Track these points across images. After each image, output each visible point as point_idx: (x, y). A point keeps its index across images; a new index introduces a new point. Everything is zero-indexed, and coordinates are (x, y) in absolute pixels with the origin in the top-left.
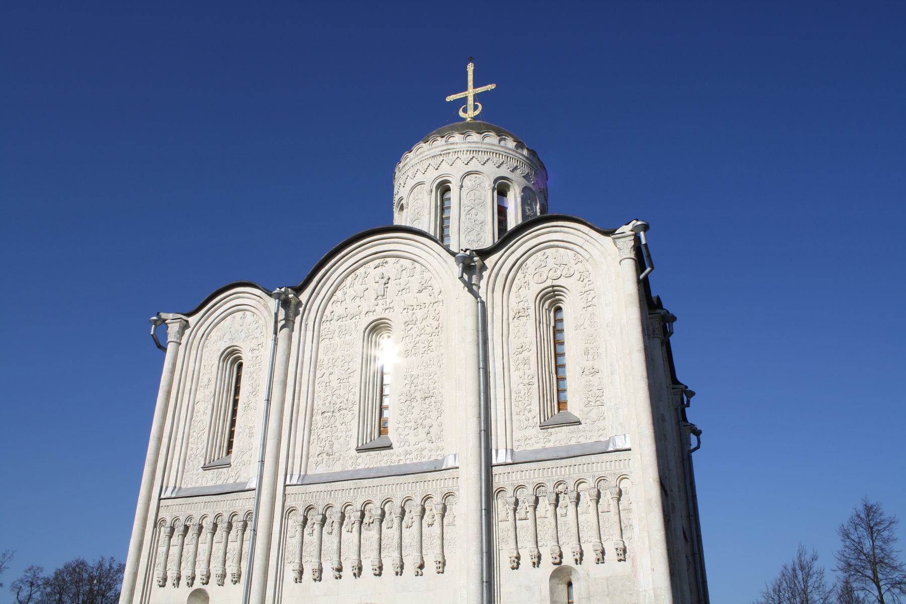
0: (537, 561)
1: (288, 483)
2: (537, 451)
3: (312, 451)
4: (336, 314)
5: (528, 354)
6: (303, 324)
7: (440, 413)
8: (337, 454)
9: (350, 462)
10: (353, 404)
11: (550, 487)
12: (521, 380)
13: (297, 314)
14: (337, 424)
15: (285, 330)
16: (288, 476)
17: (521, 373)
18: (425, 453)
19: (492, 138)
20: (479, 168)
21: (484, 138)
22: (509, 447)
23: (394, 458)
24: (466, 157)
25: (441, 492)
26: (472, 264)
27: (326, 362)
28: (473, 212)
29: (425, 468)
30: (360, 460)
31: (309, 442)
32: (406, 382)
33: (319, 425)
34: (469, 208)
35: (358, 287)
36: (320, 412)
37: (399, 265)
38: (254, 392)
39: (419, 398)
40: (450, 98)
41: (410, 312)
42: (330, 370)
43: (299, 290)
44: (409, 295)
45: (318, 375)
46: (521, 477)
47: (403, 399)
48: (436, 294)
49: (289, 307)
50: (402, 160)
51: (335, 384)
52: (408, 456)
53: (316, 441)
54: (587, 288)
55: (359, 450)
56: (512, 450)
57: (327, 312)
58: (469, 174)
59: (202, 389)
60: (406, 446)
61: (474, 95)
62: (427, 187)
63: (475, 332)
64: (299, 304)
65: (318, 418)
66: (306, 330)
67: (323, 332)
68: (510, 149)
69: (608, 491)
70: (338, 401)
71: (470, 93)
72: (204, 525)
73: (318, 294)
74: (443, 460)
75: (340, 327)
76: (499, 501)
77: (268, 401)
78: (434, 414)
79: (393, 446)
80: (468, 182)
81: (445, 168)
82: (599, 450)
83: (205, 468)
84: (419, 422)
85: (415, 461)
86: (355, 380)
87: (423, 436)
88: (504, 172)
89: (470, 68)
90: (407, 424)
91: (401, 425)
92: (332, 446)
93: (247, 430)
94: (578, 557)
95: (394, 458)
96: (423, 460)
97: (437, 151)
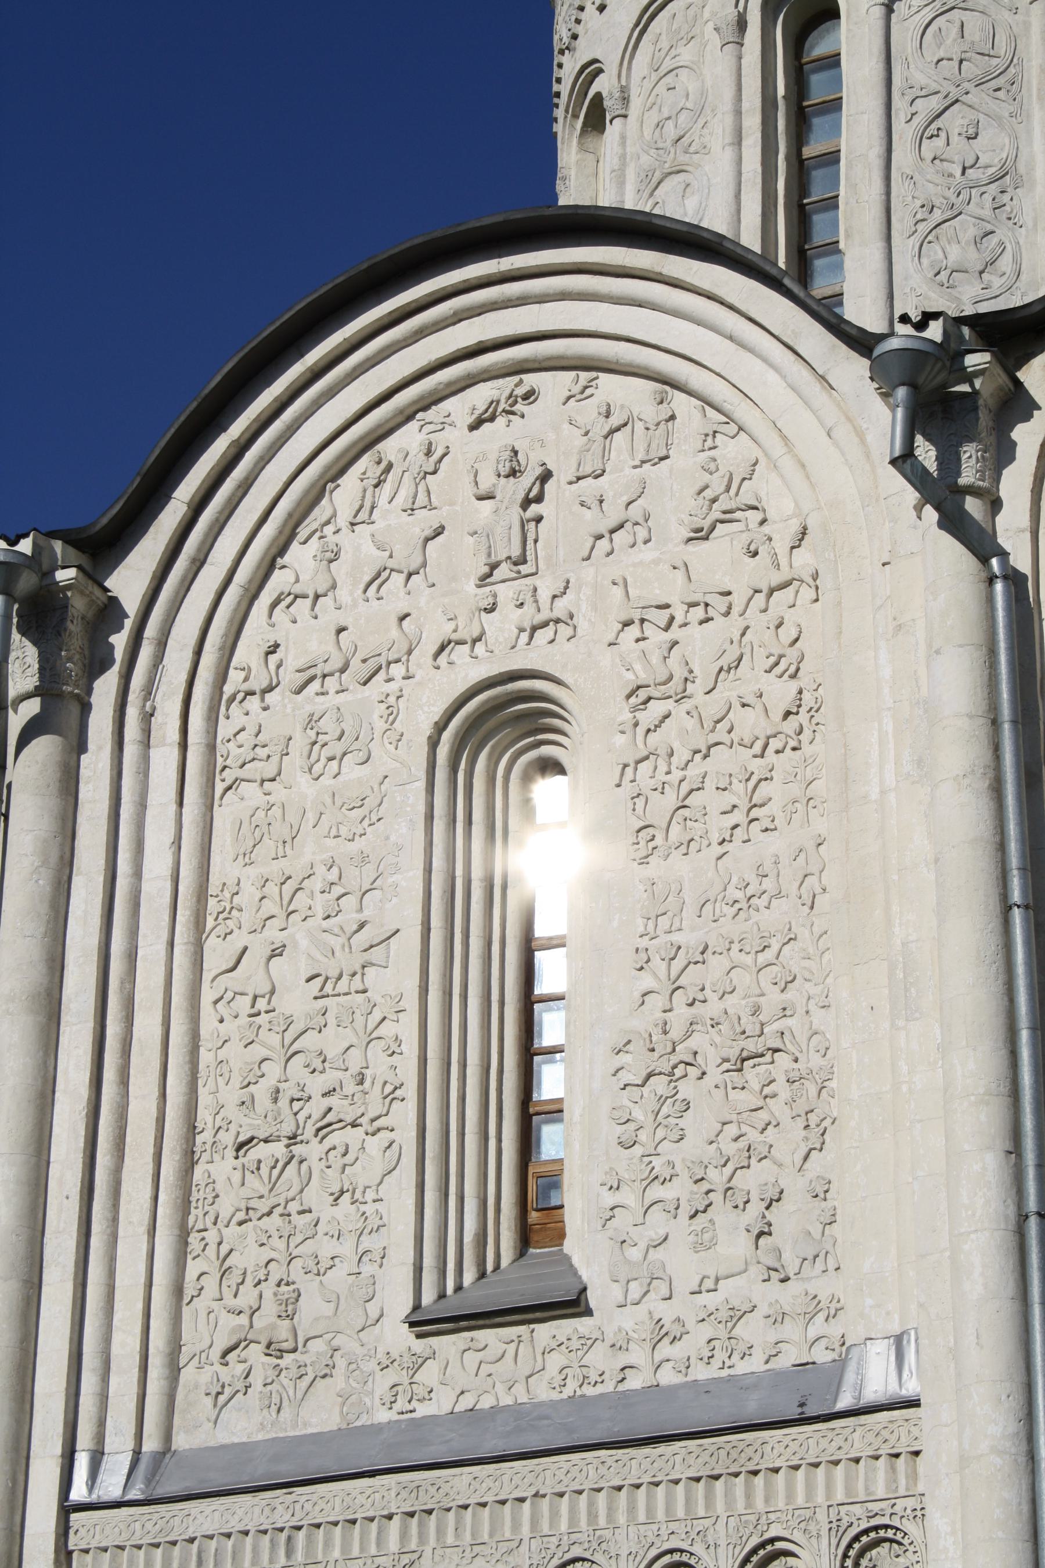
3: (193, 1336)
4: (292, 658)
6: (132, 714)
8: (316, 1346)
9: (382, 1384)
10: (391, 1097)
13: (98, 662)
14: (316, 1196)
15: (44, 749)
18: (749, 1330)
23: (598, 1358)
25: (836, 1527)
27: (249, 895)
28: (955, 121)
29: (752, 1409)
30: (428, 1375)
31: (178, 1290)
32: (647, 982)
33: (225, 1207)
34: (935, 103)
35: (396, 524)
36: (227, 1139)
37: (588, 411)
39: (710, 1058)
41: (656, 637)
42: (273, 933)
43: (105, 547)
44: (647, 554)
45: (213, 963)
48: (781, 546)
49: (59, 629)
51: (296, 1001)
52: (665, 1349)
53: (210, 1283)
55: (422, 1323)
57: (247, 652)
60: (655, 1296)
63: (980, 728)
64: (110, 612)
65: (218, 1169)
66: (146, 743)
67: (231, 752)
70: (316, 1085)
73: (199, 563)
74: (840, 1364)
75: (311, 721)
78: (787, 1143)
79: (593, 1299)
84: (717, 1178)
85: (701, 1373)
86: (397, 976)
90: (657, 1191)
91: (628, 1197)
92: (288, 1310)
95: (598, 1358)
96: (742, 1367)
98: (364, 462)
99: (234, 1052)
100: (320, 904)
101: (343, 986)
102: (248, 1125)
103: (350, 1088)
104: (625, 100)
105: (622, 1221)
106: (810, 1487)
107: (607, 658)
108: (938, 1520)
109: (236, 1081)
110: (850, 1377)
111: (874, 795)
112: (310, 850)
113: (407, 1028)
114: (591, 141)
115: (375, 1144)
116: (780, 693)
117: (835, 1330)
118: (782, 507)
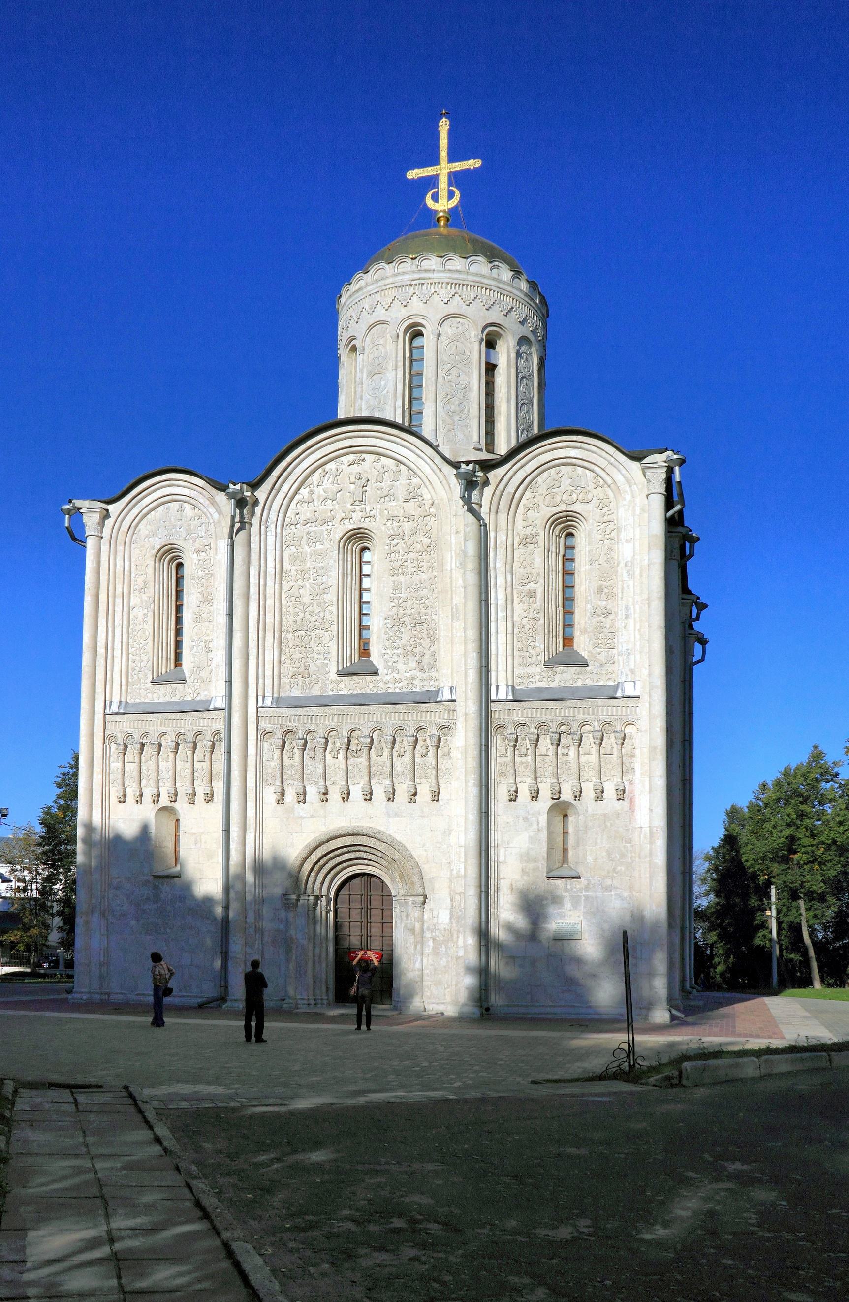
0: (535, 796)
1: (260, 704)
2: (540, 690)
5: (535, 586)
7: (433, 641)
8: (314, 677)
9: (330, 687)
10: (331, 624)
11: (553, 727)
12: (525, 614)
16: (260, 698)
17: (525, 607)
19: (480, 266)
20: (464, 309)
21: (471, 263)
22: (510, 683)
24: (445, 292)
25: (436, 724)
26: (474, 477)
29: (418, 698)
30: (342, 685)
32: (393, 604)
34: (449, 366)
36: (290, 629)
40: (413, 174)
46: (522, 715)
50: (354, 281)
52: (397, 685)
53: (288, 661)
55: (340, 674)
56: (513, 687)
58: (449, 317)
59: (137, 593)
60: (393, 673)
61: (449, 174)
62: (390, 331)
68: (504, 283)
69: (612, 735)
71: (444, 169)
74: (438, 691)
76: (498, 736)
77: (230, 615)
78: (426, 643)
79: (380, 672)
80: (448, 329)
81: (416, 306)
82: (606, 694)
85: (405, 690)
87: (413, 664)
88: (495, 316)
89: (444, 126)
90: (395, 651)
91: (388, 651)
93: (202, 644)
94: (577, 794)
95: (381, 685)
96: (414, 690)
97: (406, 278)
99: (291, 609)
101: (318, 597)
102: (295, 627)
103: (321, 621)
104: (364, 350)
106: (430, 716)
109: (292, 616)
110: (440, 694)
111: (449, 568)
113: (334, 608)
114: (351, 355)
115: (327, 634)
117: (436, 684)
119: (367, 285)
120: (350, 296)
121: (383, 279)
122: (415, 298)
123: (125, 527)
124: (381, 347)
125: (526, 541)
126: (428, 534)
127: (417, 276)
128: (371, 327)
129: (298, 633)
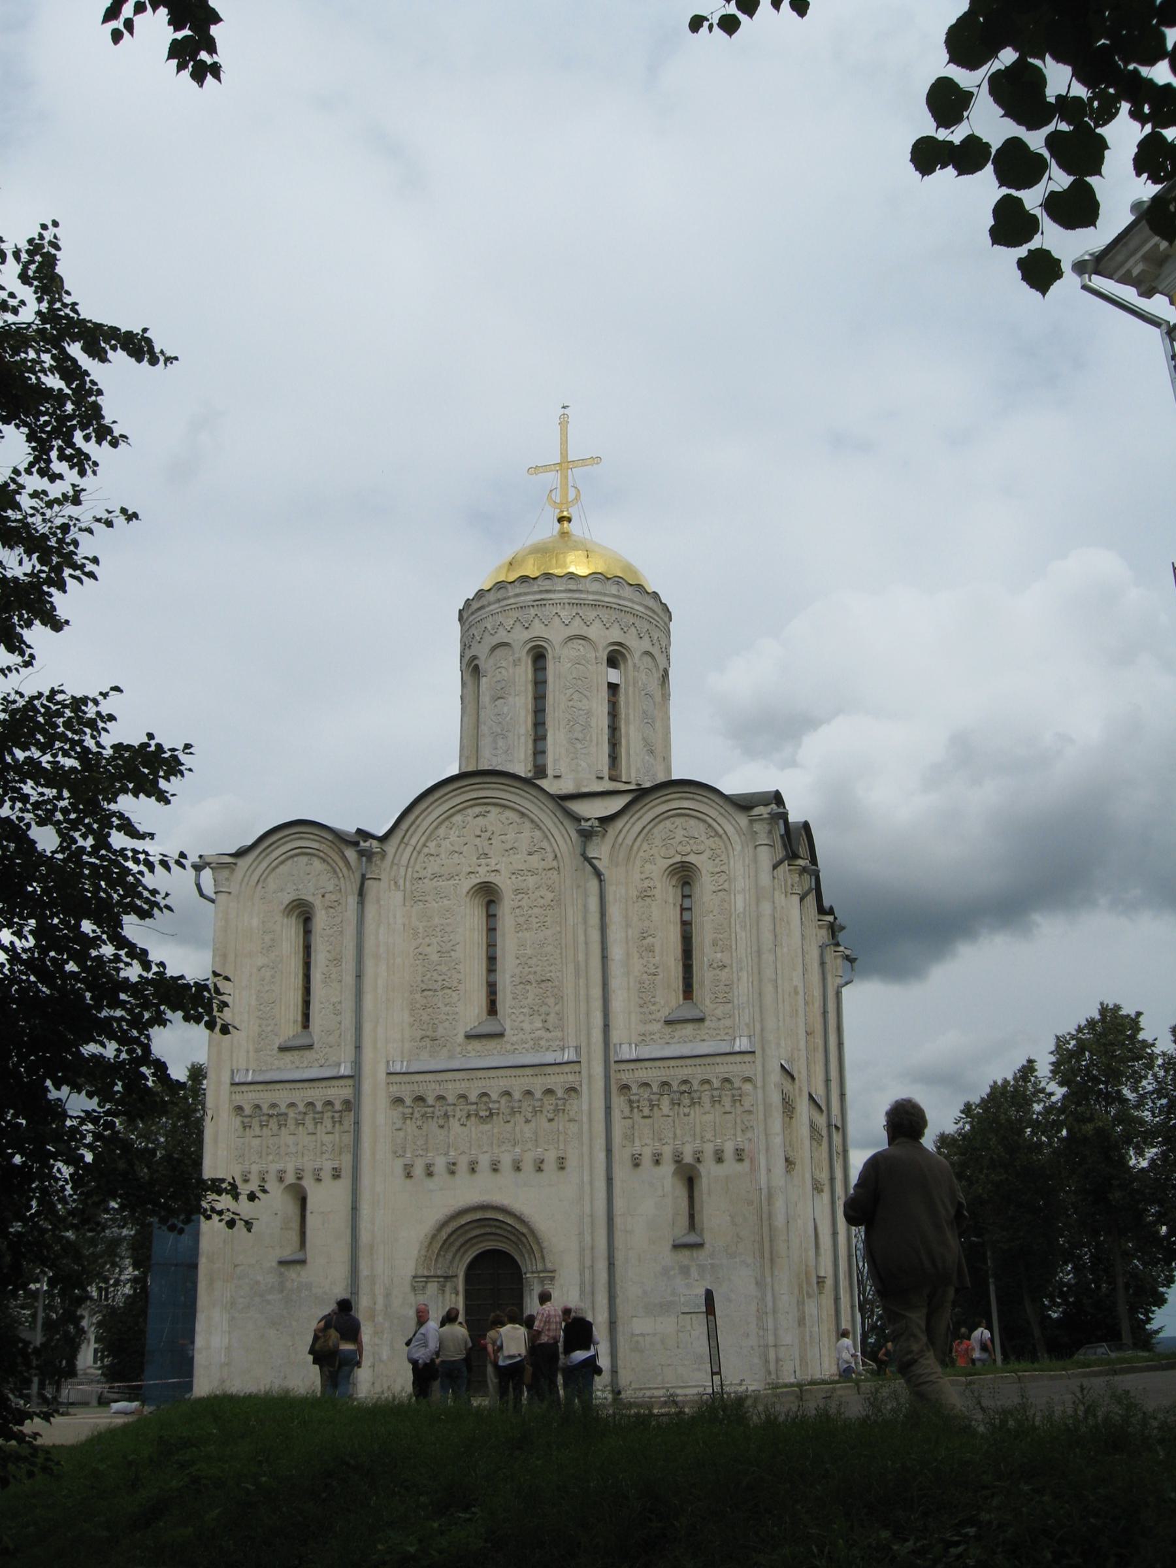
7: (559, 999)
9: (459, 1049)
10: (460, 982)
20: (584, 631)
30: (470, 1048)
37: (503, 818)
38: (337, 961)
39: (533, 981)
47: (517, 980)
51: (435, 957)
54: (718, 870)
58: (572, 638)
72: (291, 1115)
78: (551, 1001)
83: (283, 1049)
87: (540, 1025)
88: (615, 635)
93: (331, 1007)
98: (447, 823)
100: (439, 934)
102: (424, 987)
105: (513, 1016)
107: (509, 882)
108: (585, 1087)
112: (437, 921)
115: (454, 994)
116: (550, 896)
118: (549, 849)
119: (489, 604)
120: (473, 614)
121: (505, 599)
122: (537, 620)
123: (253, 882)
124: (503, 671)
125: (645, 895)
126: (550, 888)
127: (538, 597)
128: (494, 648)
129: (426, 993)
